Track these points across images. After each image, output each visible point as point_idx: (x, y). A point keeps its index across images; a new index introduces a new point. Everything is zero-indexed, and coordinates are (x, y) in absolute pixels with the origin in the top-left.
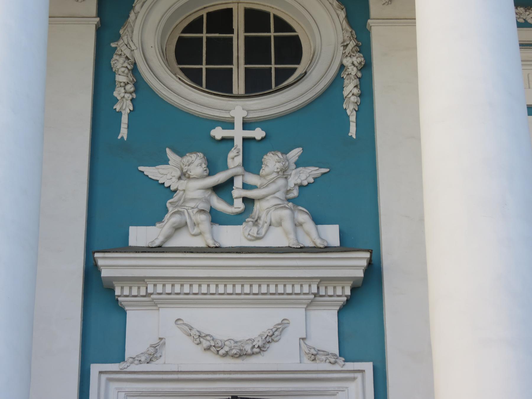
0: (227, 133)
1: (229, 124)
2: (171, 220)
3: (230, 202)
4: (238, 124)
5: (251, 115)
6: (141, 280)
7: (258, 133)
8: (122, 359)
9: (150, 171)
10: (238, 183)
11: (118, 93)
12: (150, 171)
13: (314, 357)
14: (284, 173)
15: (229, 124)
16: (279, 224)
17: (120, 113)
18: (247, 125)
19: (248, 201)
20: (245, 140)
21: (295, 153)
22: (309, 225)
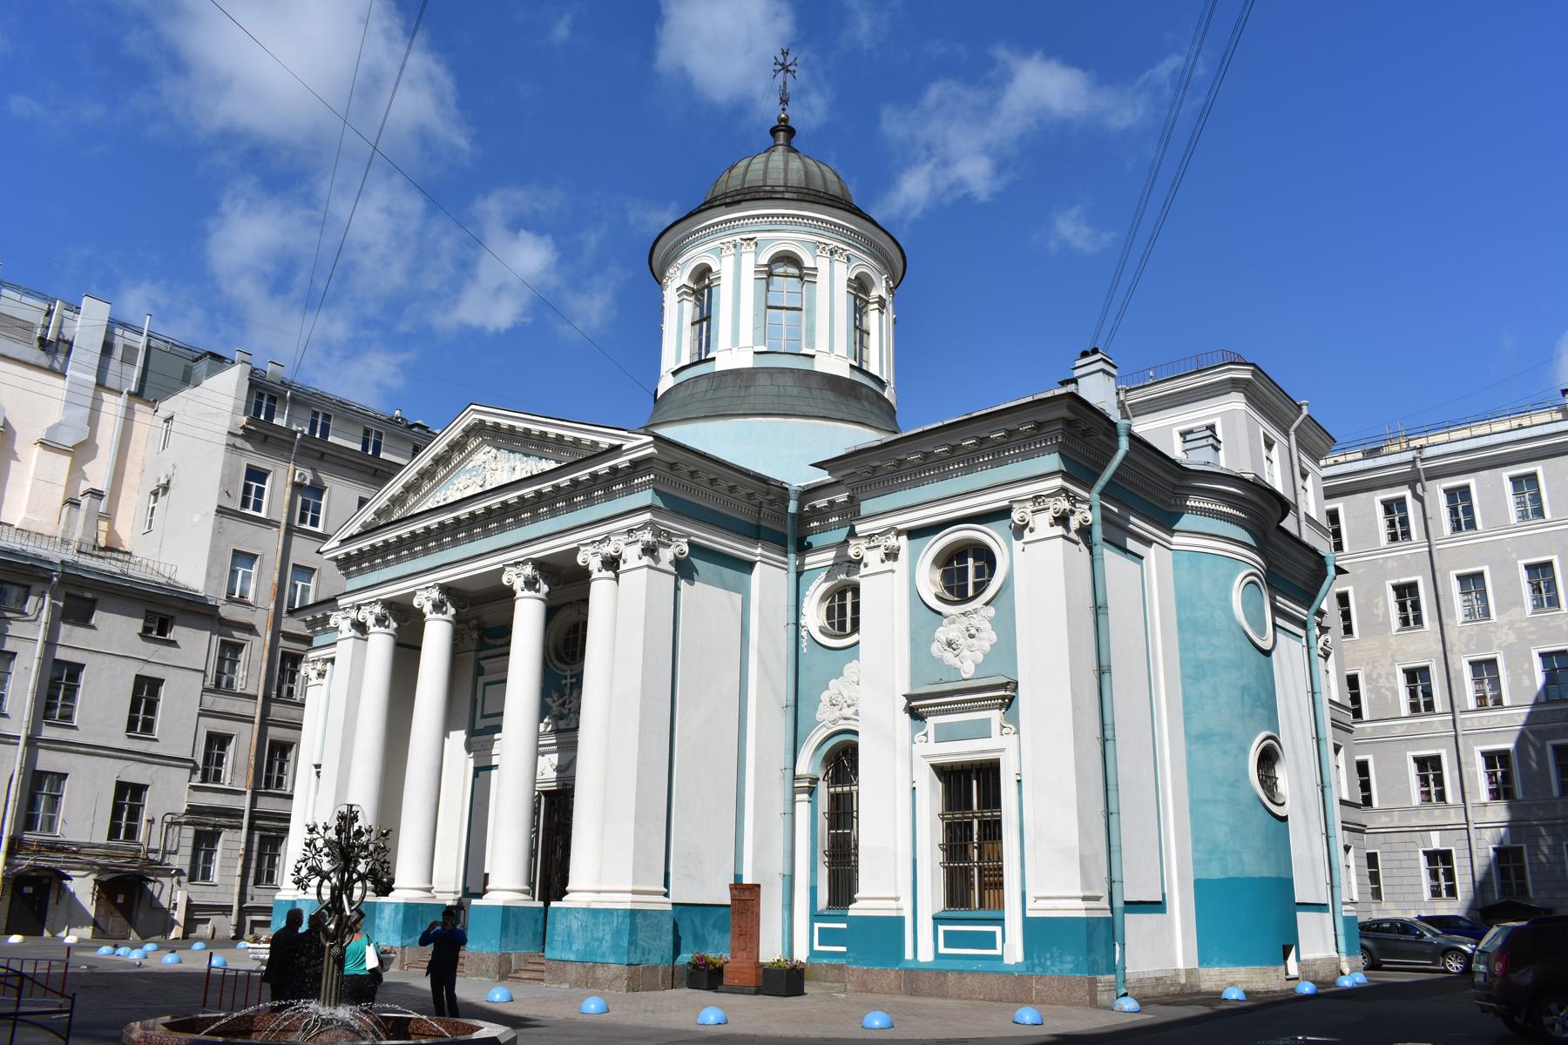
4: (569, 677)
5: (573, 673)
7: (574, 680)
10: (568, 702)
18: (571, 678)
20: (571, 683)
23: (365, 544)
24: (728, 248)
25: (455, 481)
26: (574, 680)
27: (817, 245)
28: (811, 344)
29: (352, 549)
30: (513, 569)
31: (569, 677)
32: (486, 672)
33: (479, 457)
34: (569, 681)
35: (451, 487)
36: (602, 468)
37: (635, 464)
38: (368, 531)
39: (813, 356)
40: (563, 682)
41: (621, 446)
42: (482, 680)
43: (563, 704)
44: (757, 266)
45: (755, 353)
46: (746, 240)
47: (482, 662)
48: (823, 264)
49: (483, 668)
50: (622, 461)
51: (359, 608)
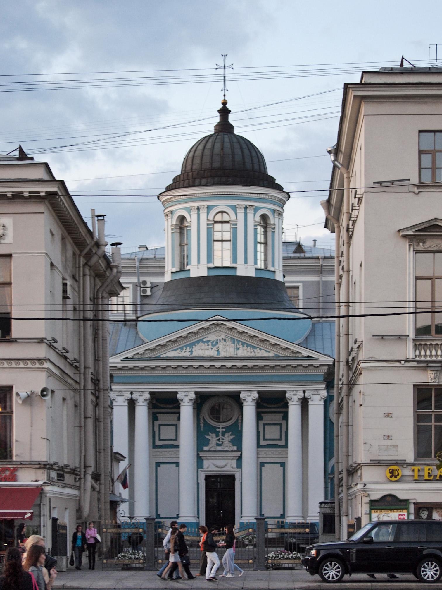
0: (219, 430)
1: (219, 428)
2: (210, 446)
3: (220, 442)
4: (221, 428)
6: (206, 456)
7: (224, 430)
8: (203, 468)
9: (206, 436)
10: (221, 439)
11: (201, 422)
12: (206, 436)
13: (232, 468)
14: (228, 437)
15: (219, 428)
16: (227, 446)
17: (201, 426)
18: (223, 428)
19: (223, 442)
21: (230, 433)
22: (232, 447)
23: (141, 364)
24: (241, 208)
25: (196, 344)
26: (224, 430)
27: (274, 211)
28: (273, 266)
29: (131, 364)
30: (245, 392)
31: (221, 428)
32: (159, 418)
33: (212, 337)
34: (221, 430)
35: (194, 346)
36: (305, 364)
37: (320, 365)
38: (140, 357)
39: (275, 272)
40: (218, 430)
41: (317, 359)
42: (157, 423)
43: (219, 440)
44: (255, 221)
45: (256, 269)
46: (250, 206)
47: (158, 415)
48: (277, 220)
49: (157, 417)
50: (316, 364)
51: (132, 393)
